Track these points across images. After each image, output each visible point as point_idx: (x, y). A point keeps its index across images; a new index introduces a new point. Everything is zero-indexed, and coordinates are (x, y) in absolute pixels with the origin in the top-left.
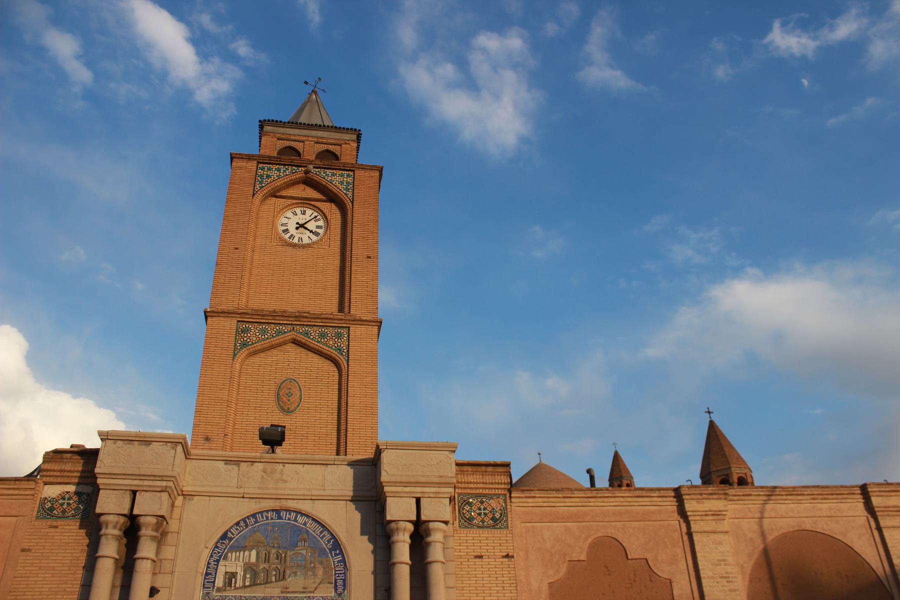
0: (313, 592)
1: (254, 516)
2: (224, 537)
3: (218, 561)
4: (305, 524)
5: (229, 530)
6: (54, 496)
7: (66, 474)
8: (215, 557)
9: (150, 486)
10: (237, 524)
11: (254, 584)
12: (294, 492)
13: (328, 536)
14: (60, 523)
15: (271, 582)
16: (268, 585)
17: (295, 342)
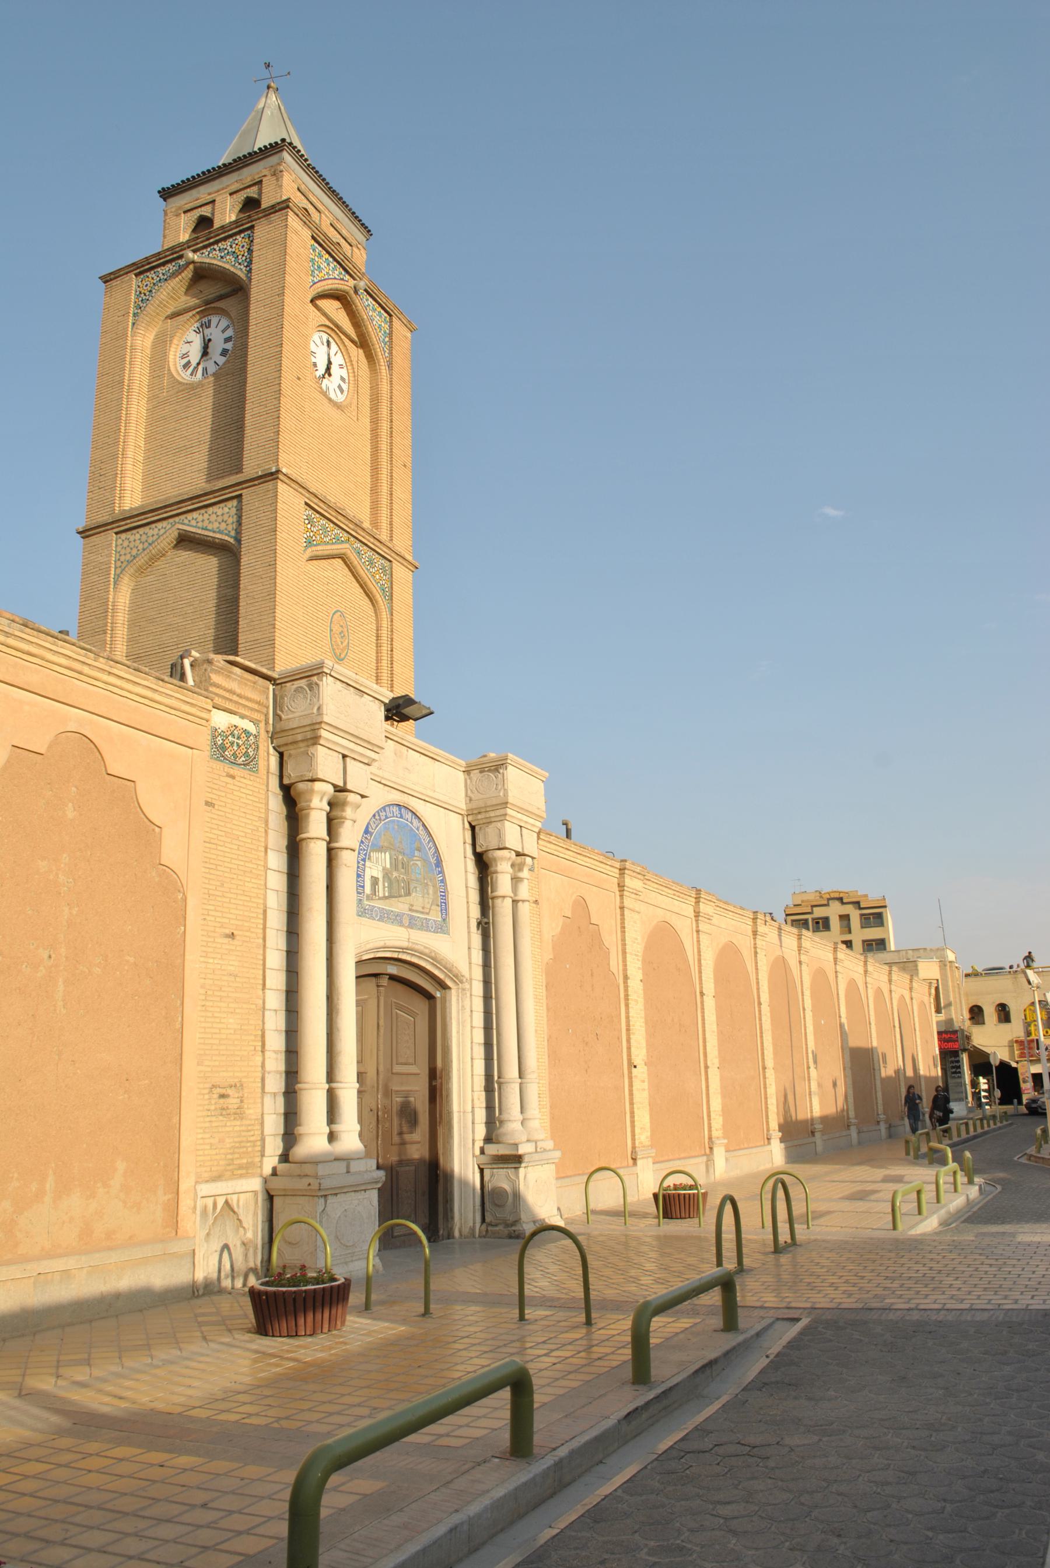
0: (428, 914)
1: (384, 808)
2: (367, 831)
3: (364, 860)
4: (418, 829)
5: (369, 823)
6: (223, 728)
7: (235, 698)
8: (362, 856)
9: (362, 754)
10: (374, 816)
11: (390, 897)
12: (416, 788)
13: (433, 850)
14: (236, 771)
15: (400, 896)
16: (401, 899)
17: (343, 557)
